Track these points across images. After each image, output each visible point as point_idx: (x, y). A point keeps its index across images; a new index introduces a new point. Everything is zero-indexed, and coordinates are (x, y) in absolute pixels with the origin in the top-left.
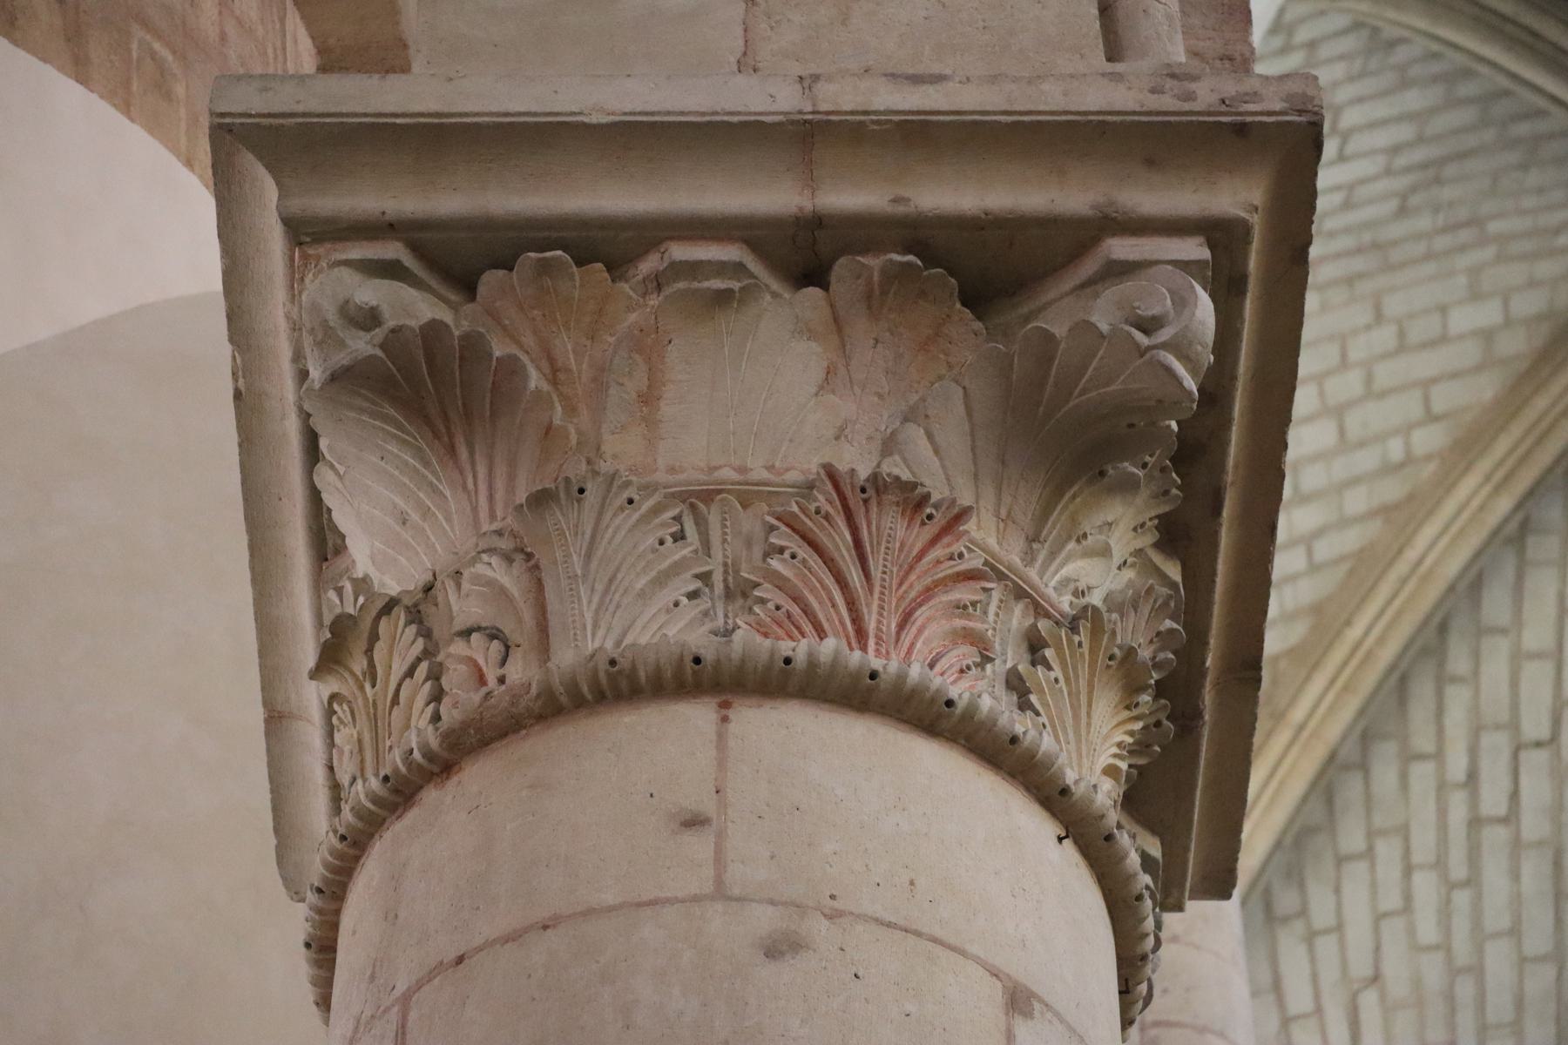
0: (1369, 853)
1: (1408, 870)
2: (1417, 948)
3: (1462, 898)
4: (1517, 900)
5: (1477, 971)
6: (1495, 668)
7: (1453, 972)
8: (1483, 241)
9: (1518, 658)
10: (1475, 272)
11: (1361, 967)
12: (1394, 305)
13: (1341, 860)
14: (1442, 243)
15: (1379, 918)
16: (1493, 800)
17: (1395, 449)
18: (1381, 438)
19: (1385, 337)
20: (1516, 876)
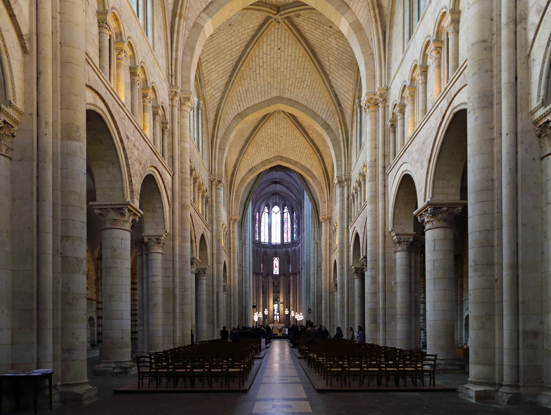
0: (247, 78)
1: (250, 80)
2: (252, 87)
3: (255, 82)
4: (260, 81)
5: (257, 88)
6: (257, 60)
7: (255, 88)
8: (251, 19)
9: (259, 58)
10: (251, 22)
11: (247, 89)
12: (243, 26)
13: (244, 79)
14: (247, 19)
15: (248, 84)
16: (258, 73)
17: (246, 40)
18: (244, 39)
19: (243, 29)
20: (260, 79)
